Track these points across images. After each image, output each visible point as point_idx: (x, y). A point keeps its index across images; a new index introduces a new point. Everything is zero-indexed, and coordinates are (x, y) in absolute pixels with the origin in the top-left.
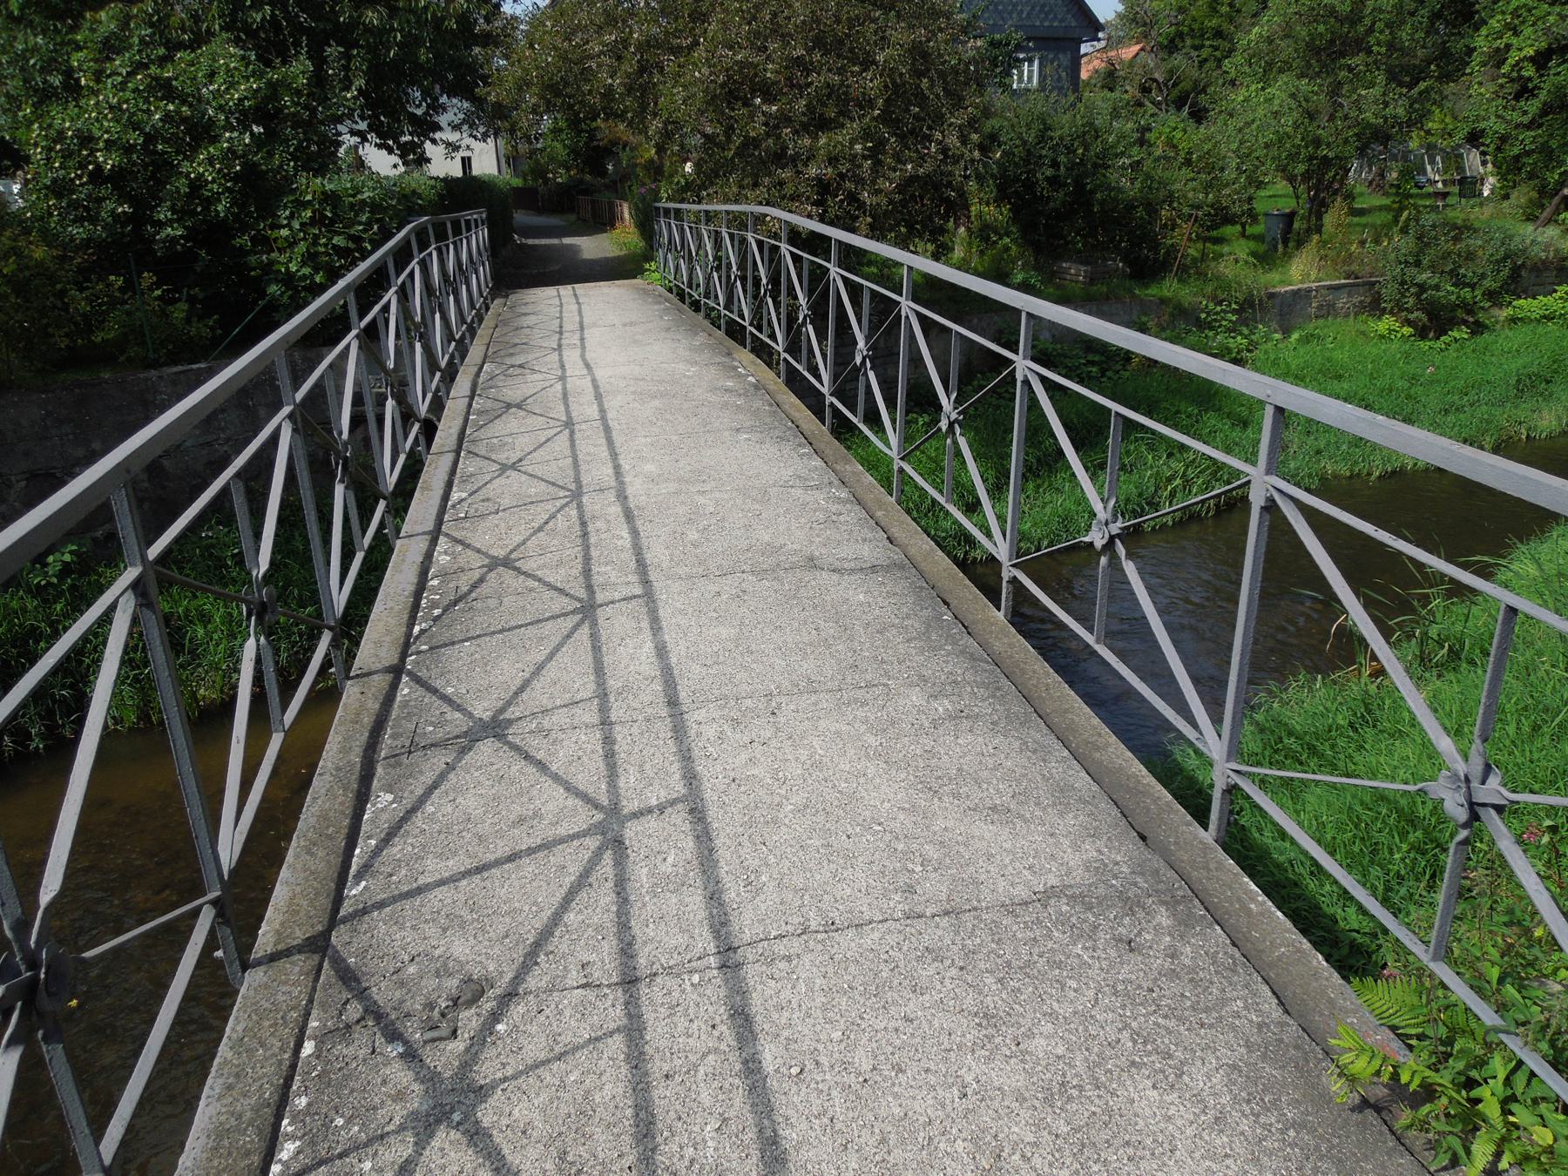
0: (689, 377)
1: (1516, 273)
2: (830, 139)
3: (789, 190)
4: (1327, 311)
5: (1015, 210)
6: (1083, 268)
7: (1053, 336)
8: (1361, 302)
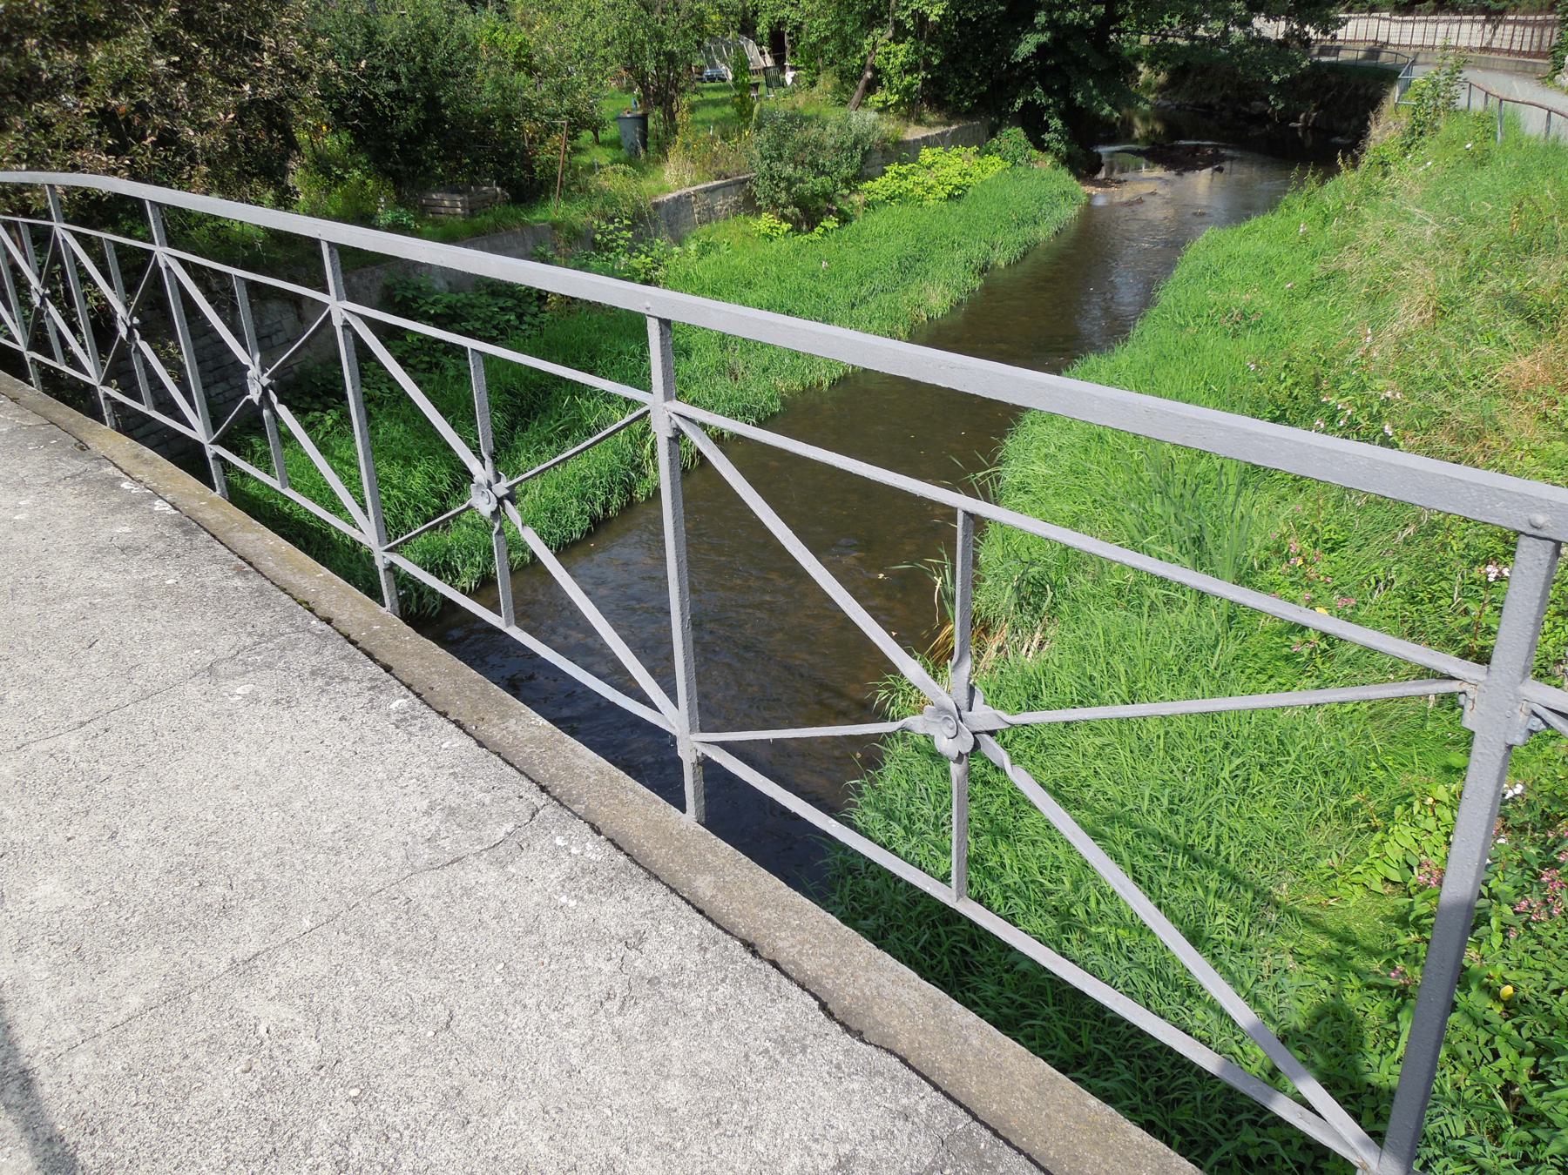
0: (28, 527)
1: (866, 155)
2: (110, 53)
3: (61, 133)
4: (710, 215)
5: (357, 134)
6: (459, 198)
7: (449, 283)
8: (736, 202)
